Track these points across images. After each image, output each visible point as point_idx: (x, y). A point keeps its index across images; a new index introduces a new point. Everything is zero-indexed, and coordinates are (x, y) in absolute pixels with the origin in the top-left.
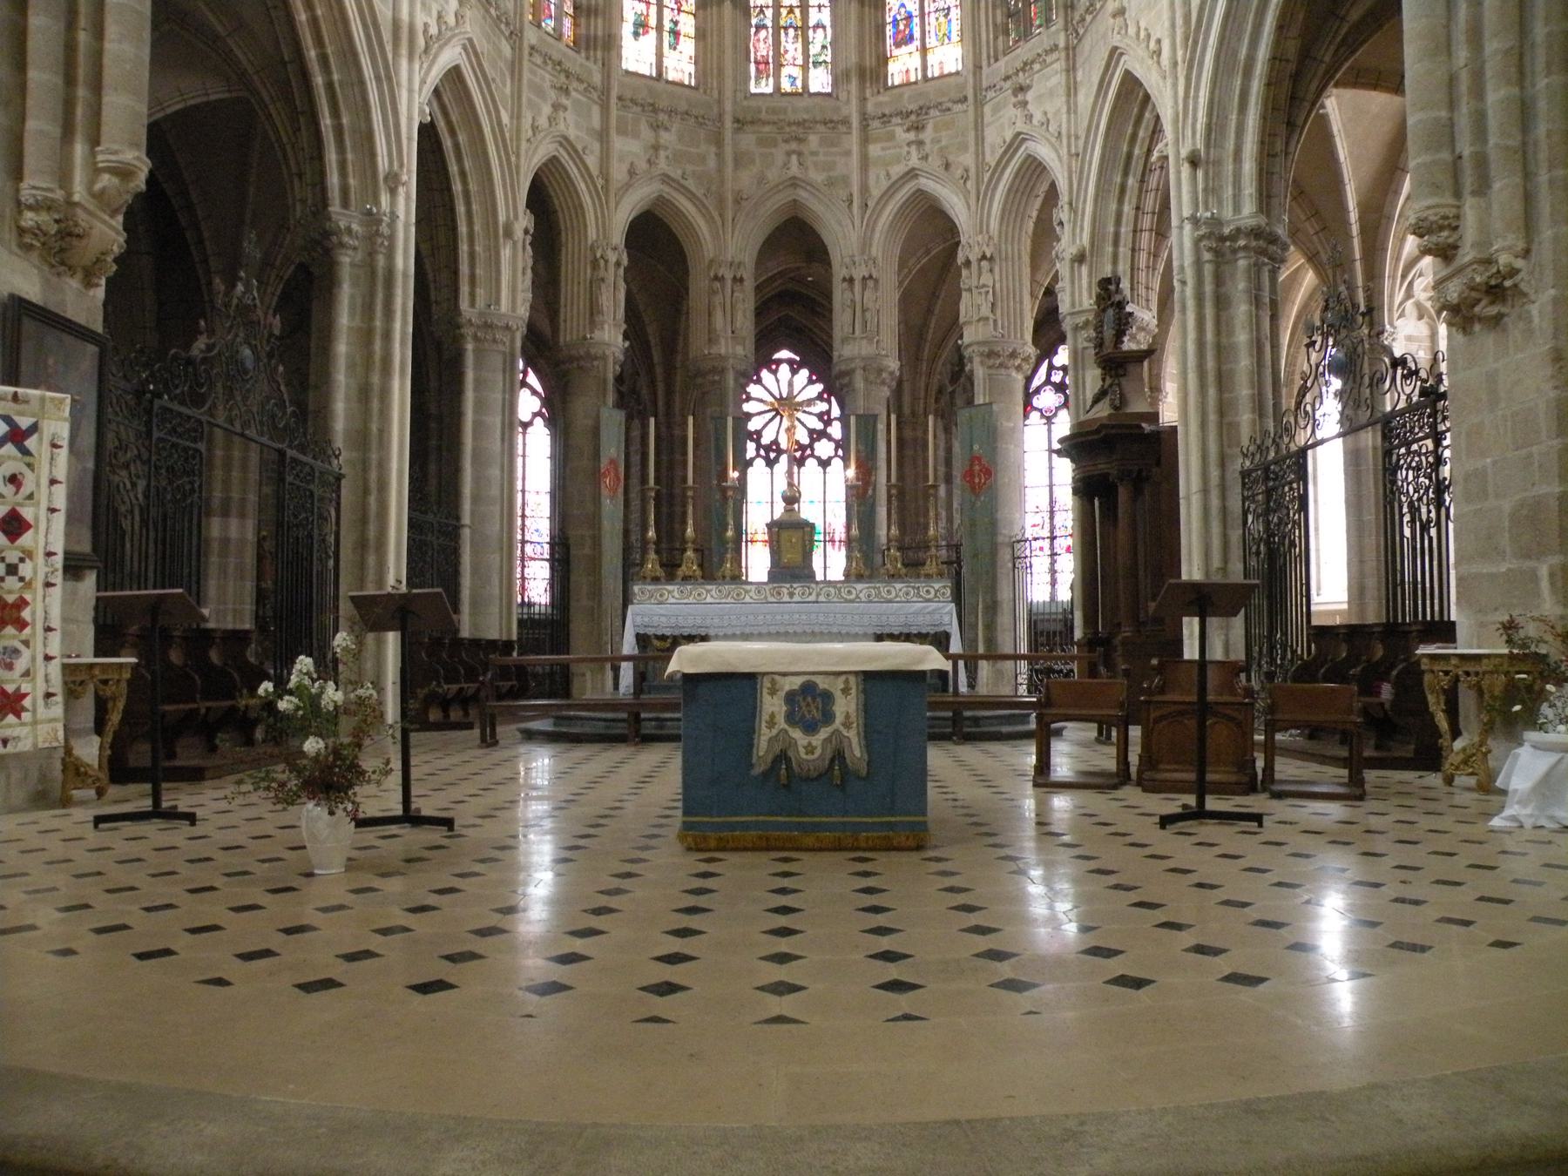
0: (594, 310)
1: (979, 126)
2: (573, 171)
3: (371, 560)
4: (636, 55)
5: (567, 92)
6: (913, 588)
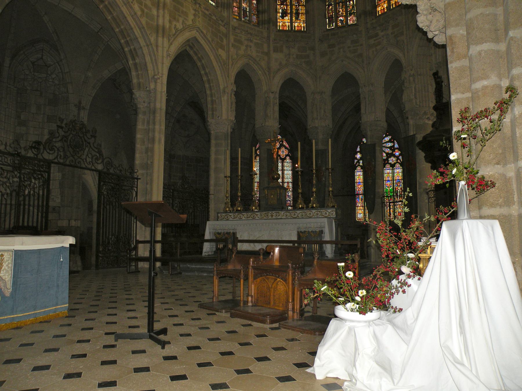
4: (284, 23)
5: (251, 41)
6: (320, 212)
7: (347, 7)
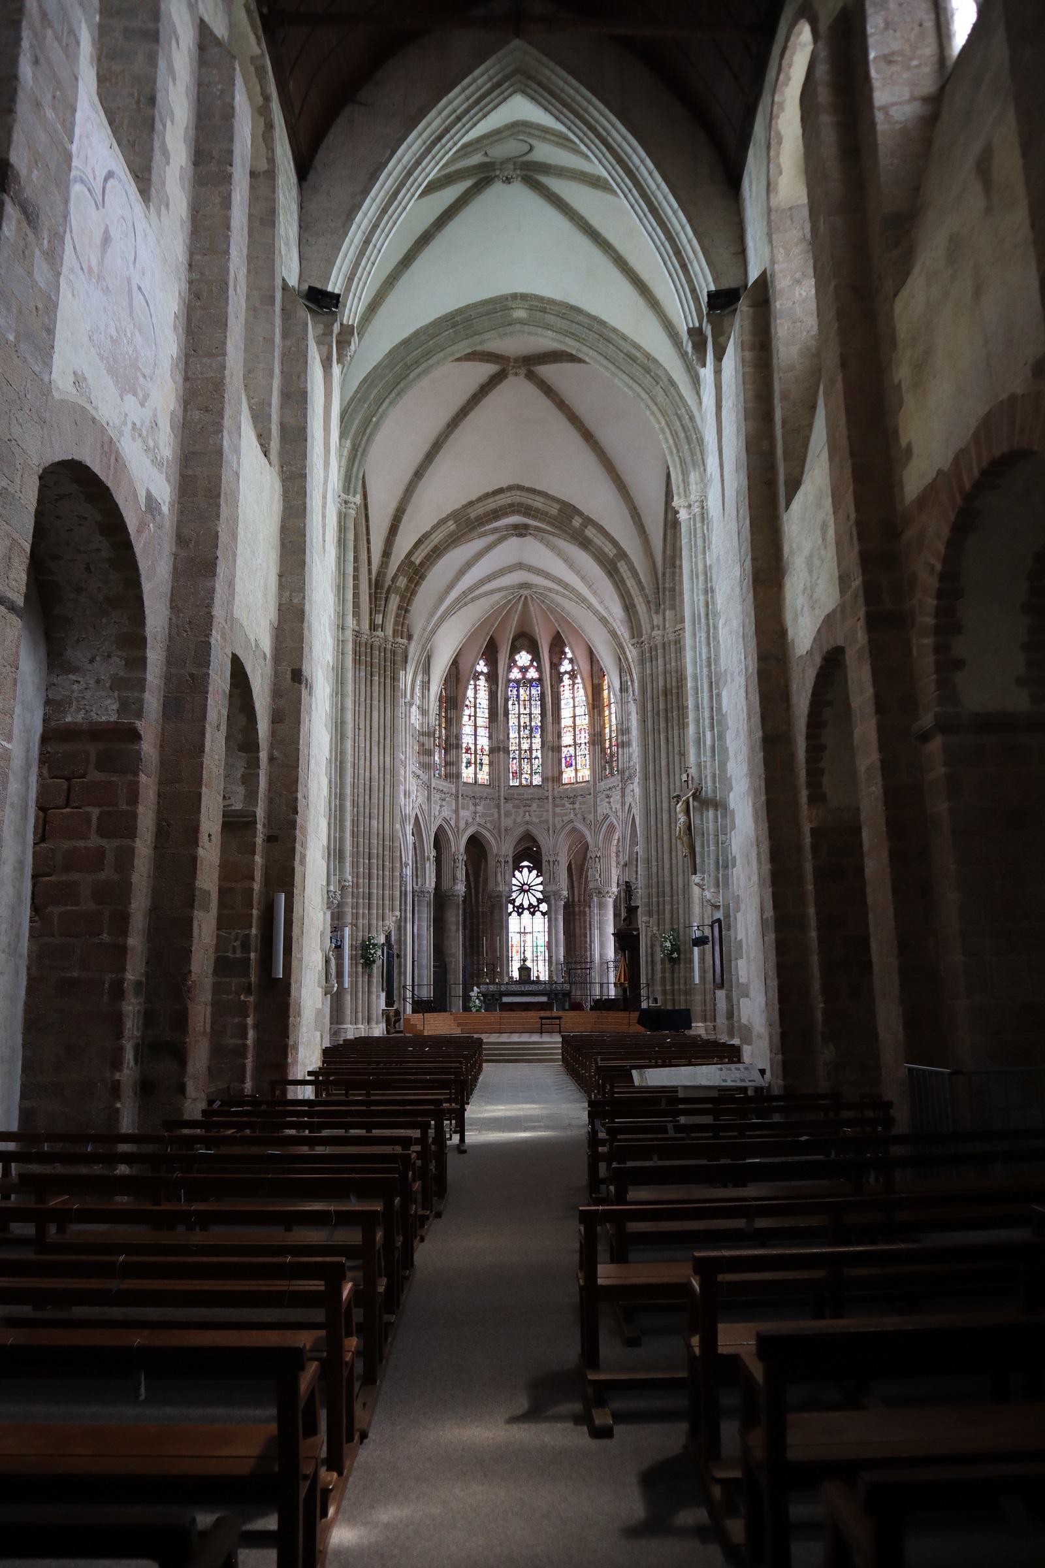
0: (454, 878)
1: (595, 806)
2: (446, 827)
3: (402, 978)
7: (532, 765)
